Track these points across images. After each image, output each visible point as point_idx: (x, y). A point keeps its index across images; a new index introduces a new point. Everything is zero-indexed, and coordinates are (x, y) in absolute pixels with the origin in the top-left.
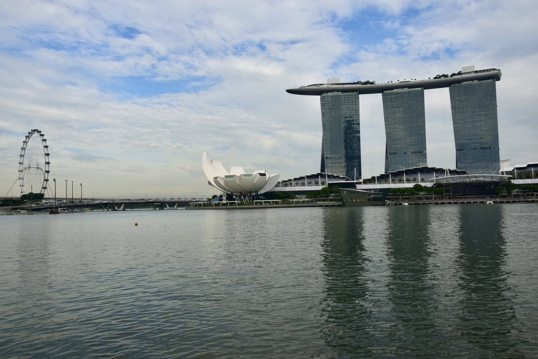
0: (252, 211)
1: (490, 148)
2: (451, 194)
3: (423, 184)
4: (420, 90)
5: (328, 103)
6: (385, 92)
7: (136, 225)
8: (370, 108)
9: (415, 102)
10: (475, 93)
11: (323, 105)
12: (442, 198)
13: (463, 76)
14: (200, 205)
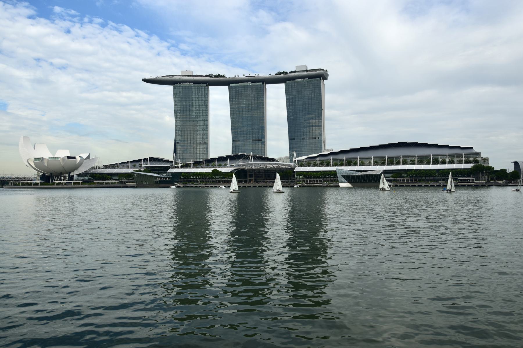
2: (253, 178)
3: (220, 169)
5: (180, 93)
6: (231, 85)
10: (306, 89)
12: (246, 182)
13: (296, 74)
14: (23, 184)
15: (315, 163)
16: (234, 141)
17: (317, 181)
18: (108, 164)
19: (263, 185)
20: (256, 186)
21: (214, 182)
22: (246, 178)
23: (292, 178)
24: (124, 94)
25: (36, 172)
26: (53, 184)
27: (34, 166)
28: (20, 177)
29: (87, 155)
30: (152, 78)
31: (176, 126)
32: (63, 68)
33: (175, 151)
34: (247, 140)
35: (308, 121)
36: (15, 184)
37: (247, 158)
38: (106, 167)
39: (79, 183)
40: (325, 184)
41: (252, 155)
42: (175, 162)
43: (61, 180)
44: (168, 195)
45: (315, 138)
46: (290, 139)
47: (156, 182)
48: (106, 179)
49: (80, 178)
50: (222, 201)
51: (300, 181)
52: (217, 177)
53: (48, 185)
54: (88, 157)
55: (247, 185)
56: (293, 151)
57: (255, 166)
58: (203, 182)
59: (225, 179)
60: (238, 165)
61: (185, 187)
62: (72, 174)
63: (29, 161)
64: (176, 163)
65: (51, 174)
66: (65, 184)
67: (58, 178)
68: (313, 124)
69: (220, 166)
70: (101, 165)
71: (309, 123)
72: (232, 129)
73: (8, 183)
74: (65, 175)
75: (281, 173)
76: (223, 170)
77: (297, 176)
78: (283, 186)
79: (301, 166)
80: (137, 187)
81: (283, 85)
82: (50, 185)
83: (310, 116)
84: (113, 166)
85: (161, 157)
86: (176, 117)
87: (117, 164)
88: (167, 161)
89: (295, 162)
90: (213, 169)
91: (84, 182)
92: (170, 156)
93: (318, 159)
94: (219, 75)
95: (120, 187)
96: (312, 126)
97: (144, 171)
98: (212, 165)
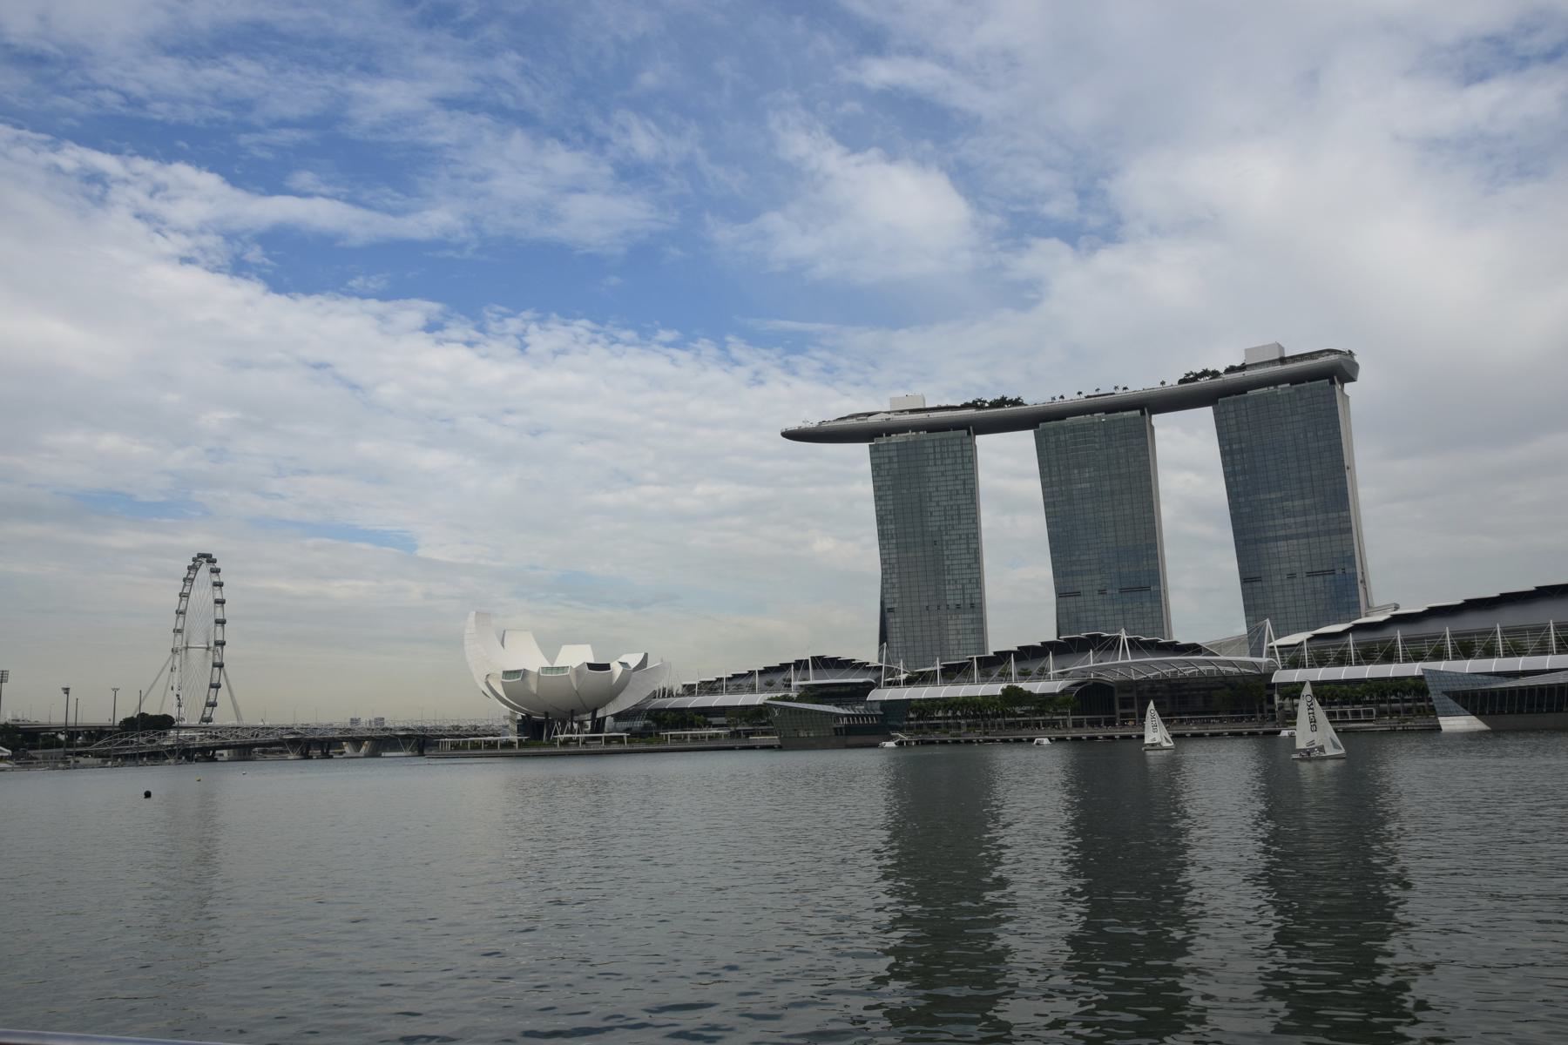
0: (707, 754)
3: (1025, 686)
4: (1134, 418)
7: (148, 795)
8: (1008, 469)
9: (1122, 450)
10: (1285, 419)
11: (876, 468)
12: (1110, 723)
15: (1343, 652)
16: (1061, 594)
17: (1356, 713)
21: (1010, 725)
22: (1110, 708)
23: (1267, 707)
25: (506, 710)
26: (552, 743)
27: (502, 693)
28: (464, 724)
30: (808, 425)
31: (884, 562)
33: (884, 637)
36: (456, 747)
37: (1109, 645)
38: (690, 690)
39: (620, 740)
40: (1387, 723)
41: (1124, 636)
42: (889, 670)
43: (571, 731)
46: (1247, 580)
47: (837, 731)
48: (692, 725)
52: (1018, 710)
53: (539, 746)
54: (643, 664)
55: (1117, 732)
57: (1138, 673)
58: (977, 726)
60: (1083, 671)
62: (600, 714)
64: (891, 672)
65: (546, 714)
67: (564, 724)
69: (1024, 675)
74: (582, 717)
76: (1037, 687)
77: (1283, 697)
79: (1295, 664)
80: (780, 748)
81: (1207, 412)
84: (710, 687)
87: (720, 680)
88: (863, 667)
89: (1271, 652)
90: (1004, 686)
91: (635, 735)
93: (1351, 638)
95: (733, 749)
97: (799, 699)
98: (1001, 675)
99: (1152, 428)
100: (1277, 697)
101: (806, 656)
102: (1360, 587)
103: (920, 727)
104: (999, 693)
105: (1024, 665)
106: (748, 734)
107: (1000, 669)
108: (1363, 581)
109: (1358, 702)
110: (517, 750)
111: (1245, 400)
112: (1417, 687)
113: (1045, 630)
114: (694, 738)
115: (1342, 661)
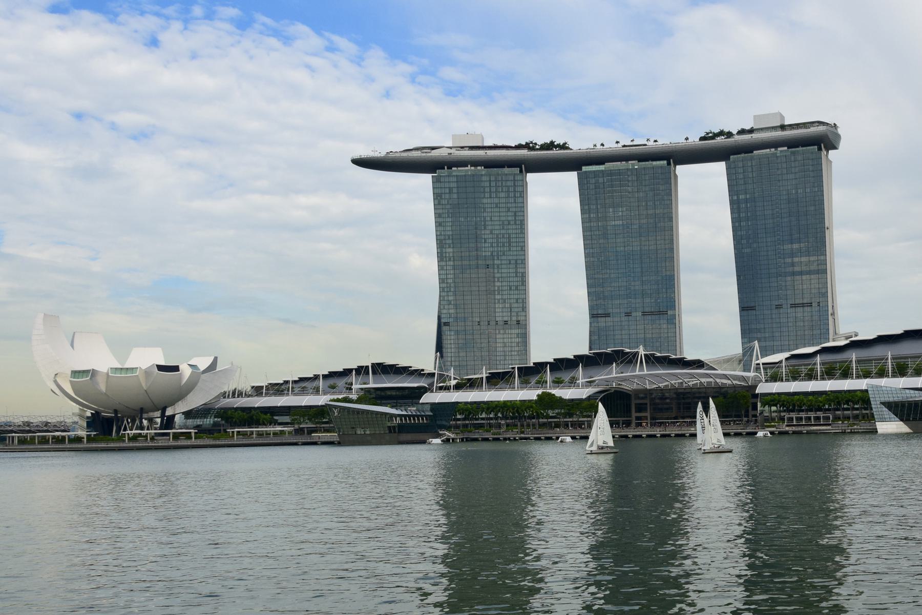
1: (810, 305)
15: (812, 370)
16: (594, 316)
17: (817, 418)
18: (264, 384)
19: (673, 431)
20: (654, 436)
21: (543, 425)
23: (751, 413)
24: (303, 200)
25: (76, 408)
26: (121, 439)
27: (70, 391)
28: (35, 420)
29: (210, 360)
31: (442, 281)
32: (141, 136)
33: (439, 347)
34: (628, 314)
35: (789, 260)
39: (188, 436)
40: (840, 426)
42: (441, 376)
43: (142, 428)
44: (425, 460)
45: (810, 305)
46: (745, 308)
49: (190, 422)
50: (567, 478)
51: (773, 420)
52: (551, 413)
53: (108, 441)
54: (212, 367)
55: (630, 433)
56: (751, 340)
59: (575, 417)
60: (607, 380)
61: (469, 440)
63: (59, 380)
64: (442, 378)
65: (116, 412)
66: (152, 439)
67: (133, 421)
68: (804, 268)
69: (558, 383)
70: (246, 385)
71: (793, 264)
72: (589, 286)
73: (4, 439)
74: (151, 414)
75: (721, 399)
76: (567, 394)
77: (764, 405)
78: (726, 435)
82: (113, 440)
83: (796, 246)
85: (403, 363)
86: (441, 257)
87: (286, 382)
88: (419, 373)
89: (757, 369)
91: (201, 431)
92: (426, 361)
94: (552, 143)
96: (801, 273)
97: (359, 401)
98: (538, 382)
99: (676, 176)
100: (759, 404)
101: (367, 362)
102: (830, 318)
103: (466, 426)
104: (535, 398)
105: (558, 375)
106: (311, 431)
107: (537, 378)
108: (833, 314)
109: (819, 409)
110: (85, 445)
111: (752, 159)
112: (862, 398)
113: (577, 344)
114: (260, 434)
115: (811, 376)
